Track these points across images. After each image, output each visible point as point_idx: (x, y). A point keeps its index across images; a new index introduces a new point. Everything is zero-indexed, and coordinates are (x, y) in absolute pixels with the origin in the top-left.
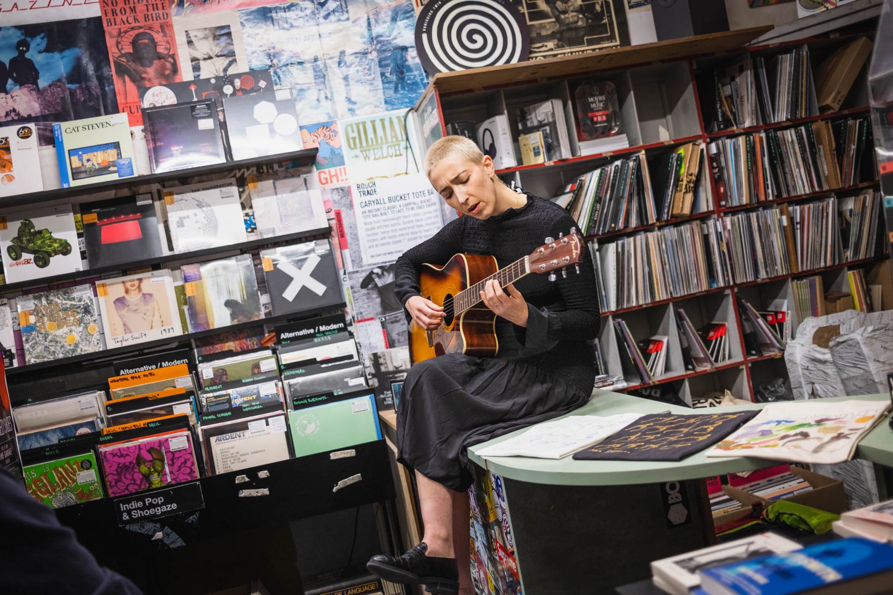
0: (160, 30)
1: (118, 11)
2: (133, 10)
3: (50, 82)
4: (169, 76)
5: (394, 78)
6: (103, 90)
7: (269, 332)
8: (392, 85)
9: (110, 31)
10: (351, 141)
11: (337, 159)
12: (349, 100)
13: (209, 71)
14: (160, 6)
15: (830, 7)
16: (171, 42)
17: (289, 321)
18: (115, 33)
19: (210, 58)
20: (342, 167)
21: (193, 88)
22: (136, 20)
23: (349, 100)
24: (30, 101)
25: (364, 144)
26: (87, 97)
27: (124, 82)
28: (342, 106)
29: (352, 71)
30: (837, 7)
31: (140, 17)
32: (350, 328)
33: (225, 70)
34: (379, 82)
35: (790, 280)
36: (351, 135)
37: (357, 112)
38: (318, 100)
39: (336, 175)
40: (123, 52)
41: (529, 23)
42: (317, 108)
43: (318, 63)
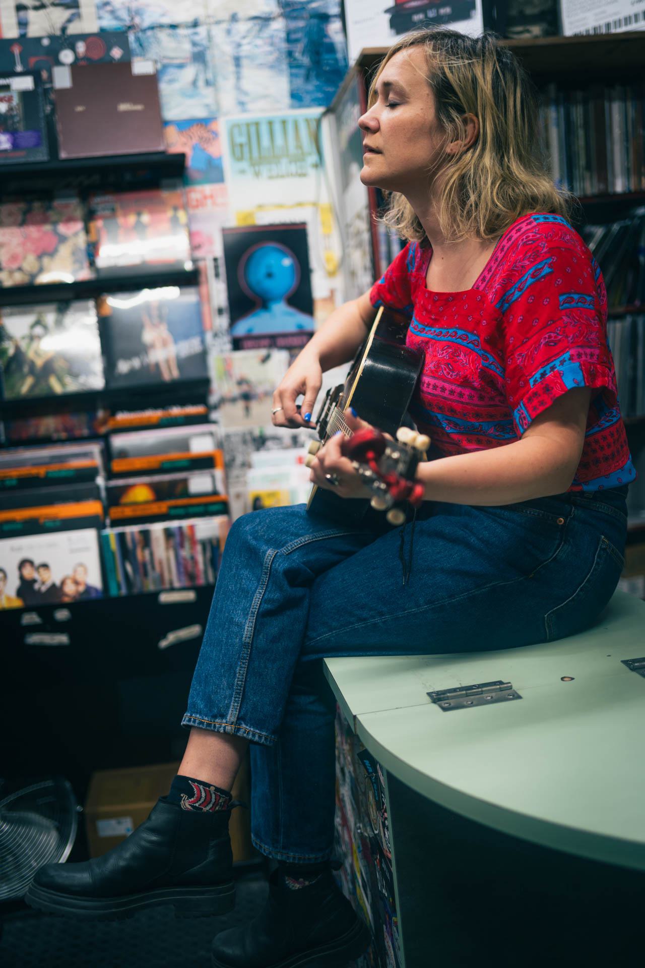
5: (306, 60)
7: (105, 408)
8: (302, 72)
10: (238, 150)
11: (215, 173)
12: (238, 88)
21: (16, 50)
32: (214, 416)
33: (64, 29)
34: (284, 66)
37: (250, 106)
38: (194, 83)
39: (212, 197)
42: (191, 96)
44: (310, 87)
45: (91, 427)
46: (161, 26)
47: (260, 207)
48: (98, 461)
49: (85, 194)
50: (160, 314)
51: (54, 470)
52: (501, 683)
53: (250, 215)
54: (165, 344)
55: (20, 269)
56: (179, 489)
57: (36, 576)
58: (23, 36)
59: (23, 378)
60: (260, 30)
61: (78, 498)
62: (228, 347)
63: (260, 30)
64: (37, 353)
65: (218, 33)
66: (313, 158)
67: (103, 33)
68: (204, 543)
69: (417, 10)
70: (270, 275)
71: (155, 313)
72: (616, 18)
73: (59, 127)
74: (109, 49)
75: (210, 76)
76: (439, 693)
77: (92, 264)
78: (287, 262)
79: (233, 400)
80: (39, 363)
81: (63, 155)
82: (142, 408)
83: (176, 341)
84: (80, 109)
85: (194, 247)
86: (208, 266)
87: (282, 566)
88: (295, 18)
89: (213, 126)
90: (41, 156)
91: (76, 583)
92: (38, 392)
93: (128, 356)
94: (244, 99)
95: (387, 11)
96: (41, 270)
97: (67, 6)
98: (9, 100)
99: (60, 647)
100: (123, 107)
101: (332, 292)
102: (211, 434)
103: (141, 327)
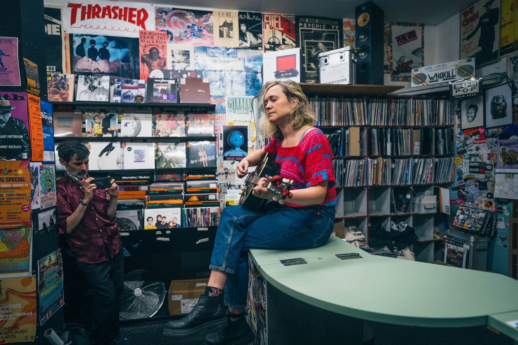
0: (161, 47)
1: (146, 37)
2: (152, 38)
3: (114, 60)
4: (162, 66)
5: (251, 83)
6: (135, 67)
7: (185, 174)
8: (249, 86)
9: (142, 44)
10: (230, 105)
11: (223, 111)
12: (232, 89)
13: (179, 67)
14: (163, 38)
15: (425, 84)
16: (165, 53)
17: (194, 170)
18: (144, 45)
19: (180, 62)
20: (224, 114)
21: (171, 73)
22: (153, 42)
23: (232, 89)
24: (105, 66)
25: (235, 107)
26: (128, 68)
27: (144, 65)
28: (228, 92)
29: (234, 79)
30: (428, 85)
31: (155, 41)
32: (217, 178)
33: (185, 69)
34: (245, 84)
35: (390, 188)
36: (230, 102)
37: (234, 94)
38: (219, 86)
39: (222, 117)
40: (145, 53)
41: (306, 71)
42: (219, 90)
43: (222, 72)
44: (251, 90)
45: (181, 179)
46: (212, 70)
47: (235, 121)
48: (183, 188)
49: (186, 113)
50: (204, 148)
51: (170, 190)
52: (301, 259)
53: (232, 123)
54: (205, 156)
55: (165, 132)
56: (206, 198)
57: (162, 220)
58: (173, 69)
59: (163, 163)
60: (239, 74)
61: (176, 199)
62: (223, 159)
63: (239, 74)
64: (168, 157)
65: (227, 74)
66: (251, 109)
67: (195, 71)
68: (212, 214)
69: (283, 73)
70: (236, 140)
71: (203, 148)
72: (335, 80)
73: (180, 94)
74: (197, 75)
75: (224, 85)
76: (283, 261)
77: (186, 132)
78: (241, 137)
79: (223, 174)
80: (168, 159)
81: (181, 102)
82: (197, 175)
83: (208, 157)
84: (187, 90)
85: (215, 131)
86: (219, 136)
87: (238, 222)
88: (249, 72)
89: (223, 98)
90: (175, 102)
91: (173, 223)
92: (167, 167)
93: (194, 159)
94: (233, 92)
95: (274, 72)
96: (171, 133)
97: (186, 63)
98: (168, 86)
99: (167, 241)
100: (199, 91)
101: (253, 146)
102: (216, 183)
103: (199, 151)
